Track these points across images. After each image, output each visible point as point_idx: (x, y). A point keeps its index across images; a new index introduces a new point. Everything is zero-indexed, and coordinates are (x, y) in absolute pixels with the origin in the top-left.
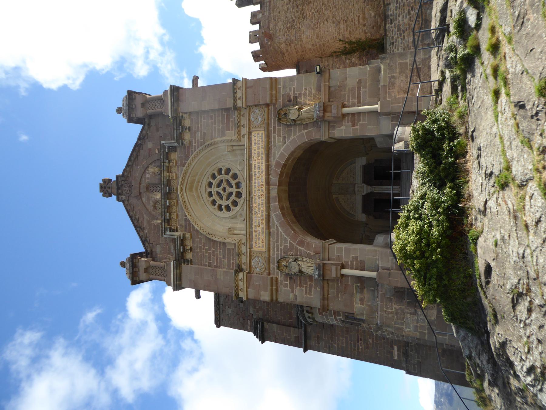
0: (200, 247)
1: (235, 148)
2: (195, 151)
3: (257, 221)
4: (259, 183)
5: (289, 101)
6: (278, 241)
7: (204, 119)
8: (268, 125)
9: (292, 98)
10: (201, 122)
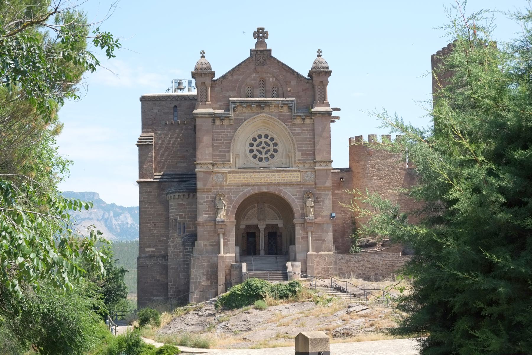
0: (224, 132)
1: (291, 159)
2: (289, 128)
3: (246, 177)
4: (269, 178)
5: (317, 198)
6: (234, 192)
7: (310, 135)
8: (304, 185)
9: (318, 200)
10: (308, 133)
